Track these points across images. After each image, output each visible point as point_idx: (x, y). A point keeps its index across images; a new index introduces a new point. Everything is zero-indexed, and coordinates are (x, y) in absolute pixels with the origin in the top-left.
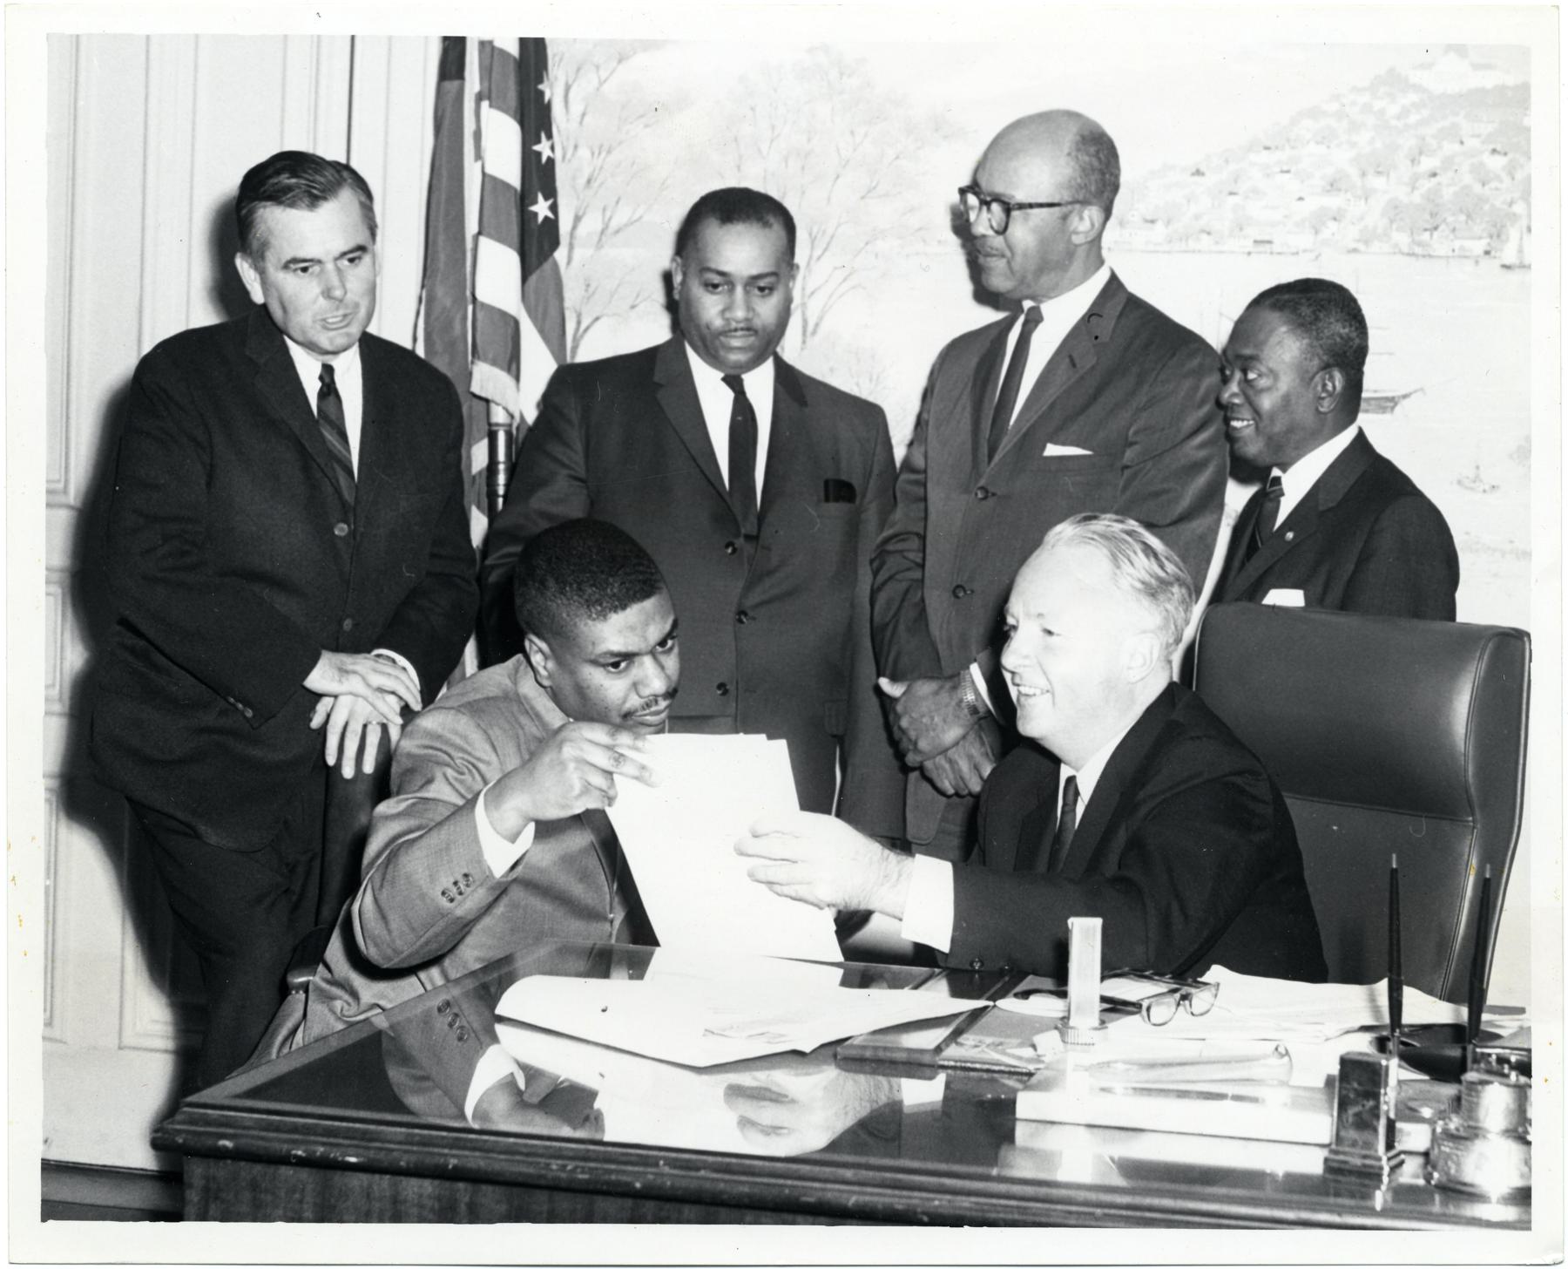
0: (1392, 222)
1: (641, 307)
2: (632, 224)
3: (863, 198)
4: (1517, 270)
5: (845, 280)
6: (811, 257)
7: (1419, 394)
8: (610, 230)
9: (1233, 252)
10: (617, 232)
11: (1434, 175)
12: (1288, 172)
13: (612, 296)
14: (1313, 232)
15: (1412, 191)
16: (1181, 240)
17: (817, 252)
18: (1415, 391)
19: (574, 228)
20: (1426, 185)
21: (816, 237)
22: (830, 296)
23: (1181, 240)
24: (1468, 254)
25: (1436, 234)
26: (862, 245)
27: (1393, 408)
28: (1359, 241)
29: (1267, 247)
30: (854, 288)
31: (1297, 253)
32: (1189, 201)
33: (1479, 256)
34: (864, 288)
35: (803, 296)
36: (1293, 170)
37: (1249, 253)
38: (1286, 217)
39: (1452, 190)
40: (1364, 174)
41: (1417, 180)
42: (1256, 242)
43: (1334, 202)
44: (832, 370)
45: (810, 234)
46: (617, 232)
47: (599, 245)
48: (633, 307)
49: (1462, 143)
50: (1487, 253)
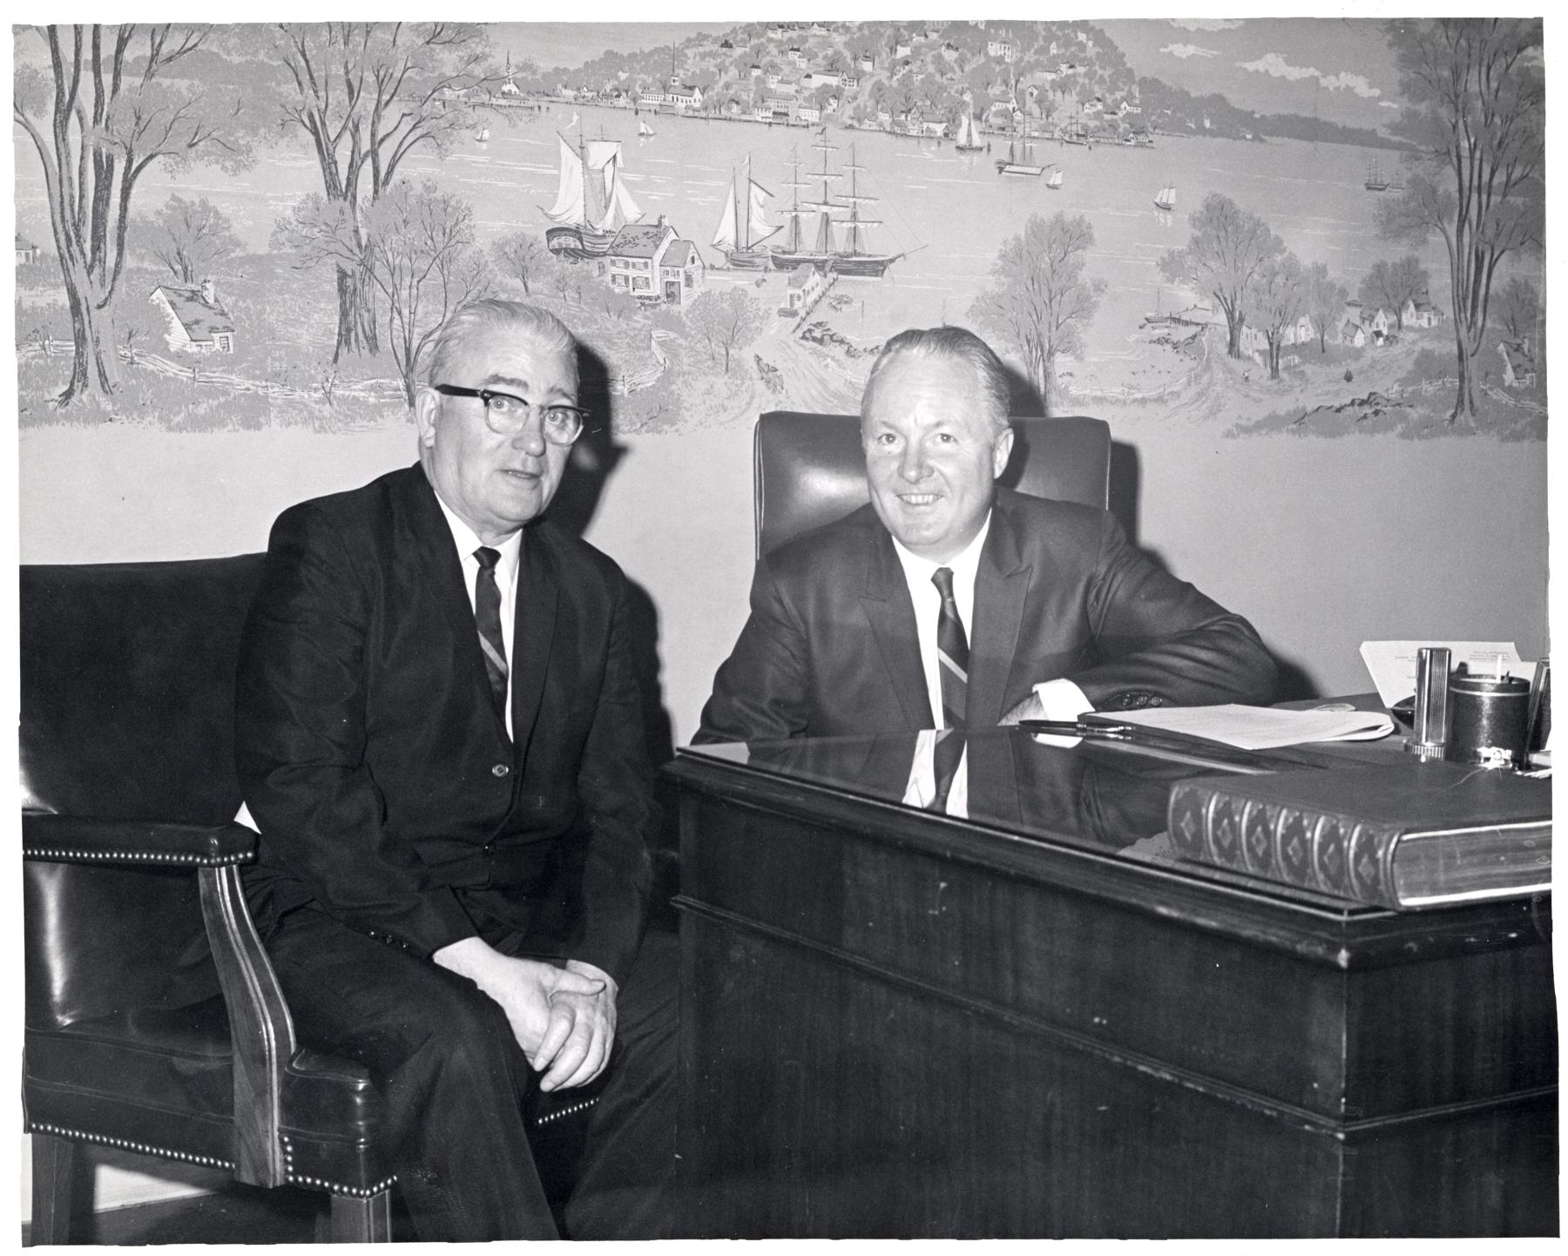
0: (878, 103)
1: (201, 144)
2: (185, 52)
3: (428, 43)
4: (968, 152)
5: (414, 127)
6: (379, 102)
7: (902, 258)
8: (161, 58)
9: (757, 122)
10: (170, 59)
11: (907, 63)
12: (798, 50)
13: (167, 133)
14: (818, 106)
15: (893, 74)
16: (715, 108)
17: (386, 97)
18: (900, 256)
19: (119, 51)
20: (904, 71)
21: (383, 80)
22: (401, 143)
23: (715, 108)
24: (932, 135)
25: (909, 118)
26: (429, 93)
27: (883, 271)
28: (853, 118)
29: (785, 118)
30: (423, 136)
31: (807, 126)
32: (720, 71)
33: (940, 137)
34: (433, 137)
35: (373, 143)
36: (801, 49)
37: (770, 124)
38: (797, 91)
39: (920, 77)
40: (855, 59)
41: (895, 67)
42: (774, 113)
43: (833, 81)
44: (405, 222)
45: (377, 77)
46: (170, 59)
47: (149, 74)
48: (191, 146)
49: (926, 36)
50: (946, 135)
